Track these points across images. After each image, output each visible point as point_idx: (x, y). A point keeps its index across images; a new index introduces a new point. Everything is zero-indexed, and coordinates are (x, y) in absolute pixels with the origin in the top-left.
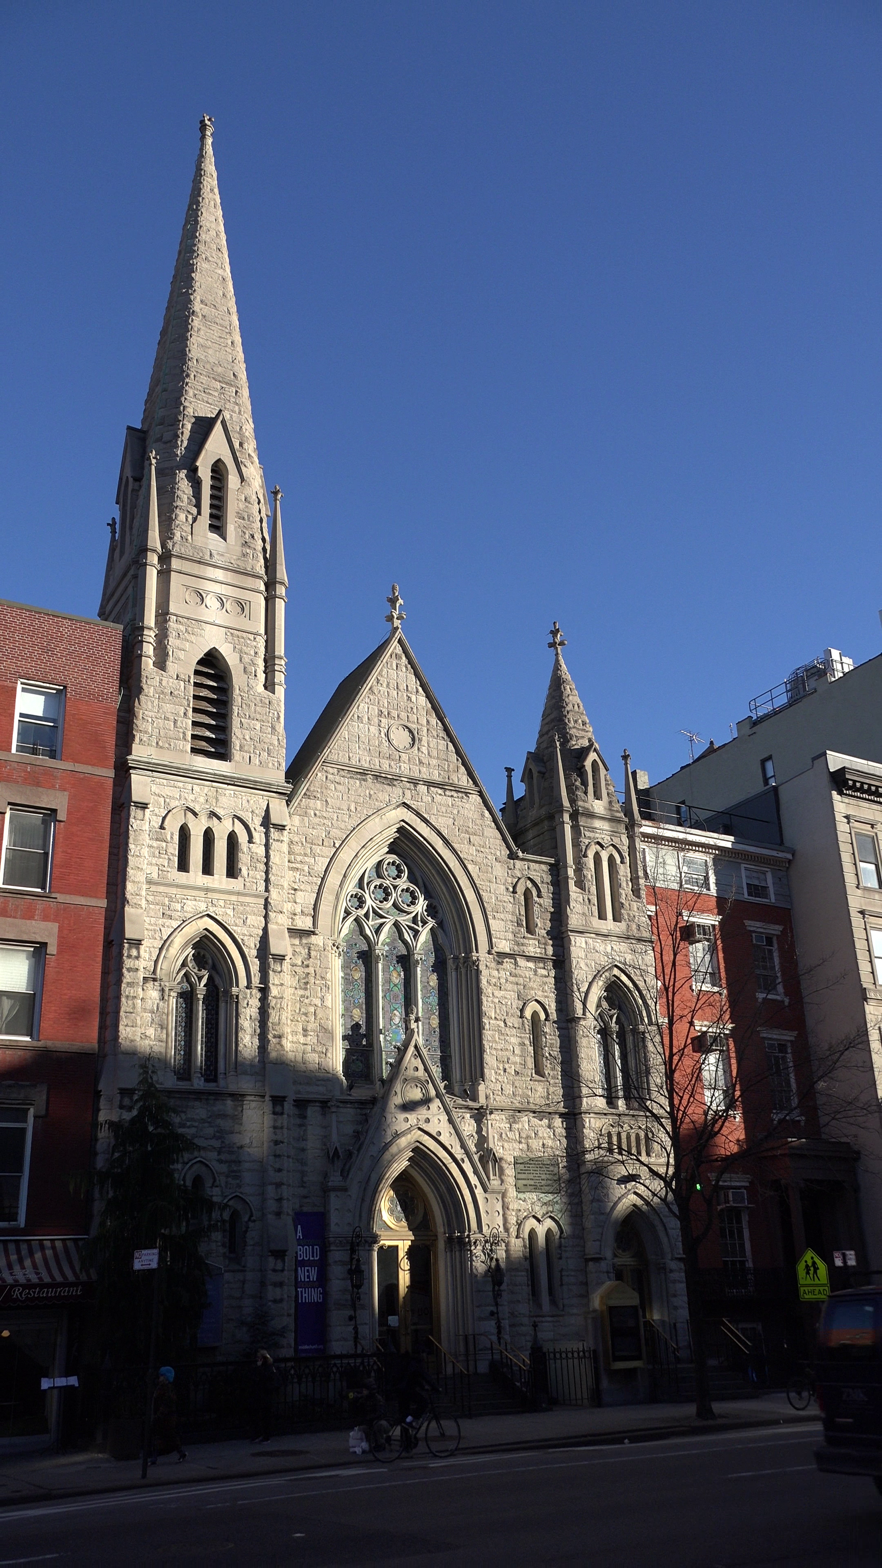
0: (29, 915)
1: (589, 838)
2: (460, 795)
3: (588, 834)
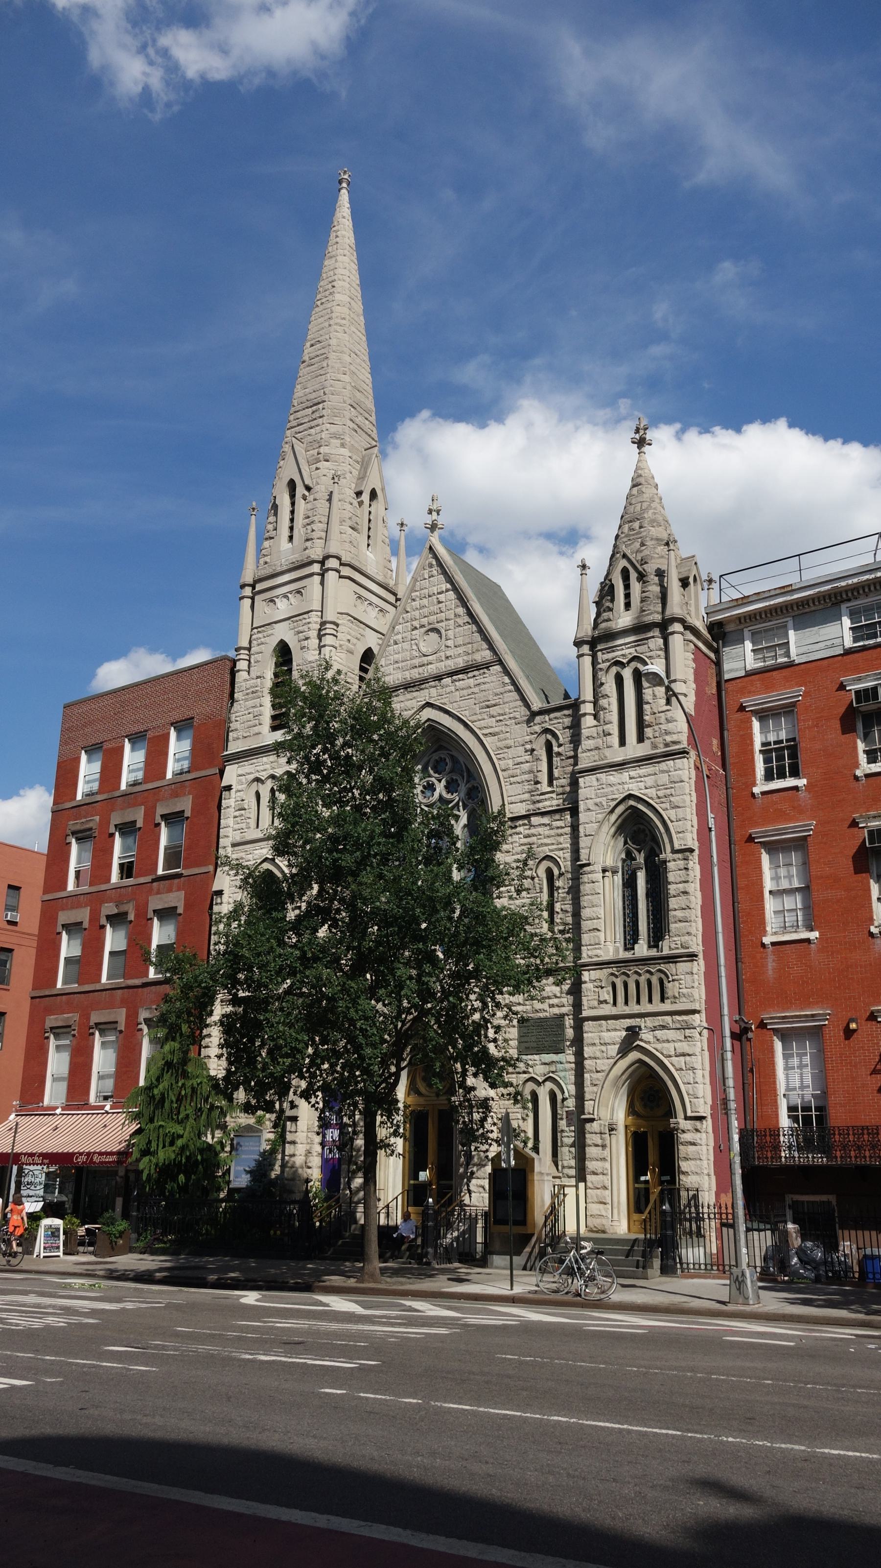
0: (170, 890)
1: (608, 660)
2: (482, 671)
3: (606, 656)
